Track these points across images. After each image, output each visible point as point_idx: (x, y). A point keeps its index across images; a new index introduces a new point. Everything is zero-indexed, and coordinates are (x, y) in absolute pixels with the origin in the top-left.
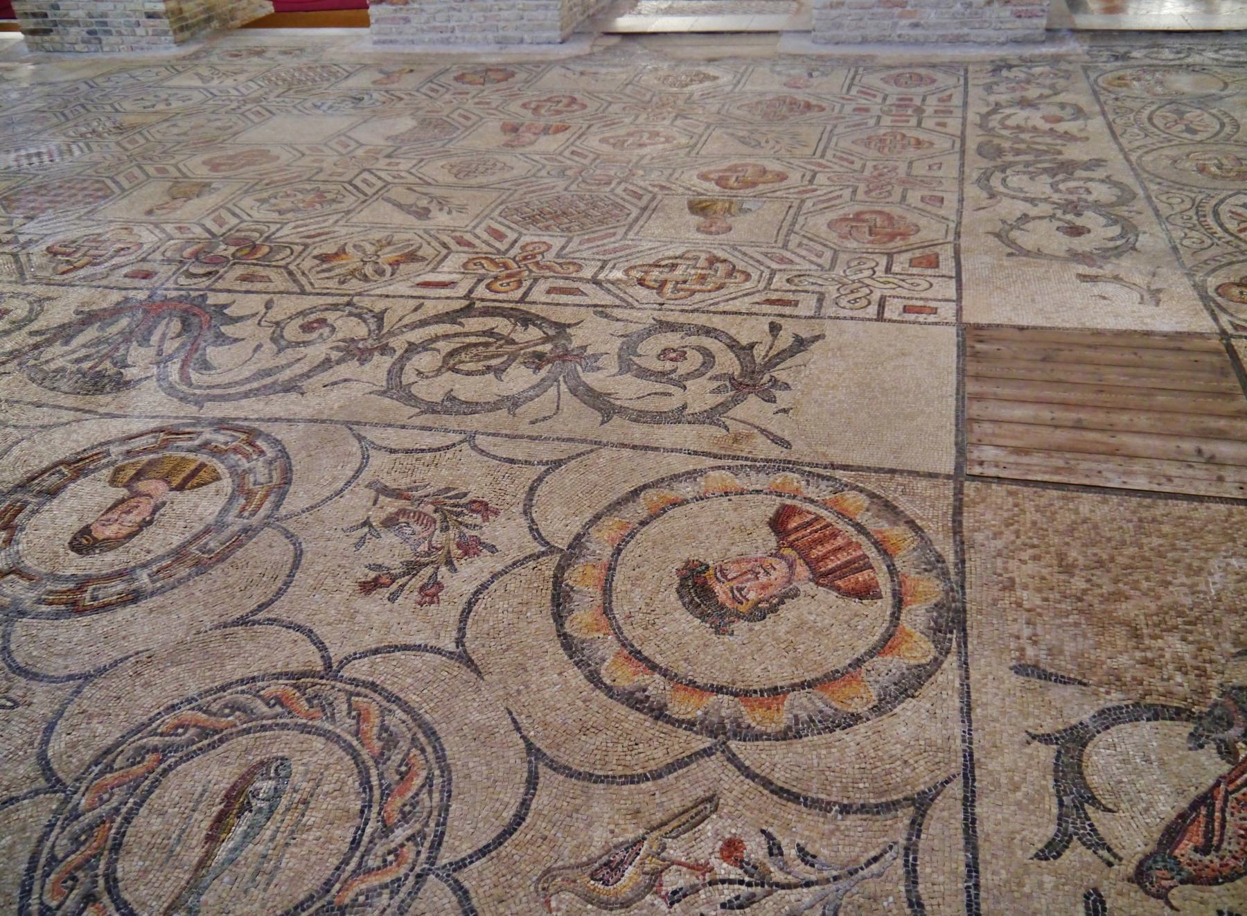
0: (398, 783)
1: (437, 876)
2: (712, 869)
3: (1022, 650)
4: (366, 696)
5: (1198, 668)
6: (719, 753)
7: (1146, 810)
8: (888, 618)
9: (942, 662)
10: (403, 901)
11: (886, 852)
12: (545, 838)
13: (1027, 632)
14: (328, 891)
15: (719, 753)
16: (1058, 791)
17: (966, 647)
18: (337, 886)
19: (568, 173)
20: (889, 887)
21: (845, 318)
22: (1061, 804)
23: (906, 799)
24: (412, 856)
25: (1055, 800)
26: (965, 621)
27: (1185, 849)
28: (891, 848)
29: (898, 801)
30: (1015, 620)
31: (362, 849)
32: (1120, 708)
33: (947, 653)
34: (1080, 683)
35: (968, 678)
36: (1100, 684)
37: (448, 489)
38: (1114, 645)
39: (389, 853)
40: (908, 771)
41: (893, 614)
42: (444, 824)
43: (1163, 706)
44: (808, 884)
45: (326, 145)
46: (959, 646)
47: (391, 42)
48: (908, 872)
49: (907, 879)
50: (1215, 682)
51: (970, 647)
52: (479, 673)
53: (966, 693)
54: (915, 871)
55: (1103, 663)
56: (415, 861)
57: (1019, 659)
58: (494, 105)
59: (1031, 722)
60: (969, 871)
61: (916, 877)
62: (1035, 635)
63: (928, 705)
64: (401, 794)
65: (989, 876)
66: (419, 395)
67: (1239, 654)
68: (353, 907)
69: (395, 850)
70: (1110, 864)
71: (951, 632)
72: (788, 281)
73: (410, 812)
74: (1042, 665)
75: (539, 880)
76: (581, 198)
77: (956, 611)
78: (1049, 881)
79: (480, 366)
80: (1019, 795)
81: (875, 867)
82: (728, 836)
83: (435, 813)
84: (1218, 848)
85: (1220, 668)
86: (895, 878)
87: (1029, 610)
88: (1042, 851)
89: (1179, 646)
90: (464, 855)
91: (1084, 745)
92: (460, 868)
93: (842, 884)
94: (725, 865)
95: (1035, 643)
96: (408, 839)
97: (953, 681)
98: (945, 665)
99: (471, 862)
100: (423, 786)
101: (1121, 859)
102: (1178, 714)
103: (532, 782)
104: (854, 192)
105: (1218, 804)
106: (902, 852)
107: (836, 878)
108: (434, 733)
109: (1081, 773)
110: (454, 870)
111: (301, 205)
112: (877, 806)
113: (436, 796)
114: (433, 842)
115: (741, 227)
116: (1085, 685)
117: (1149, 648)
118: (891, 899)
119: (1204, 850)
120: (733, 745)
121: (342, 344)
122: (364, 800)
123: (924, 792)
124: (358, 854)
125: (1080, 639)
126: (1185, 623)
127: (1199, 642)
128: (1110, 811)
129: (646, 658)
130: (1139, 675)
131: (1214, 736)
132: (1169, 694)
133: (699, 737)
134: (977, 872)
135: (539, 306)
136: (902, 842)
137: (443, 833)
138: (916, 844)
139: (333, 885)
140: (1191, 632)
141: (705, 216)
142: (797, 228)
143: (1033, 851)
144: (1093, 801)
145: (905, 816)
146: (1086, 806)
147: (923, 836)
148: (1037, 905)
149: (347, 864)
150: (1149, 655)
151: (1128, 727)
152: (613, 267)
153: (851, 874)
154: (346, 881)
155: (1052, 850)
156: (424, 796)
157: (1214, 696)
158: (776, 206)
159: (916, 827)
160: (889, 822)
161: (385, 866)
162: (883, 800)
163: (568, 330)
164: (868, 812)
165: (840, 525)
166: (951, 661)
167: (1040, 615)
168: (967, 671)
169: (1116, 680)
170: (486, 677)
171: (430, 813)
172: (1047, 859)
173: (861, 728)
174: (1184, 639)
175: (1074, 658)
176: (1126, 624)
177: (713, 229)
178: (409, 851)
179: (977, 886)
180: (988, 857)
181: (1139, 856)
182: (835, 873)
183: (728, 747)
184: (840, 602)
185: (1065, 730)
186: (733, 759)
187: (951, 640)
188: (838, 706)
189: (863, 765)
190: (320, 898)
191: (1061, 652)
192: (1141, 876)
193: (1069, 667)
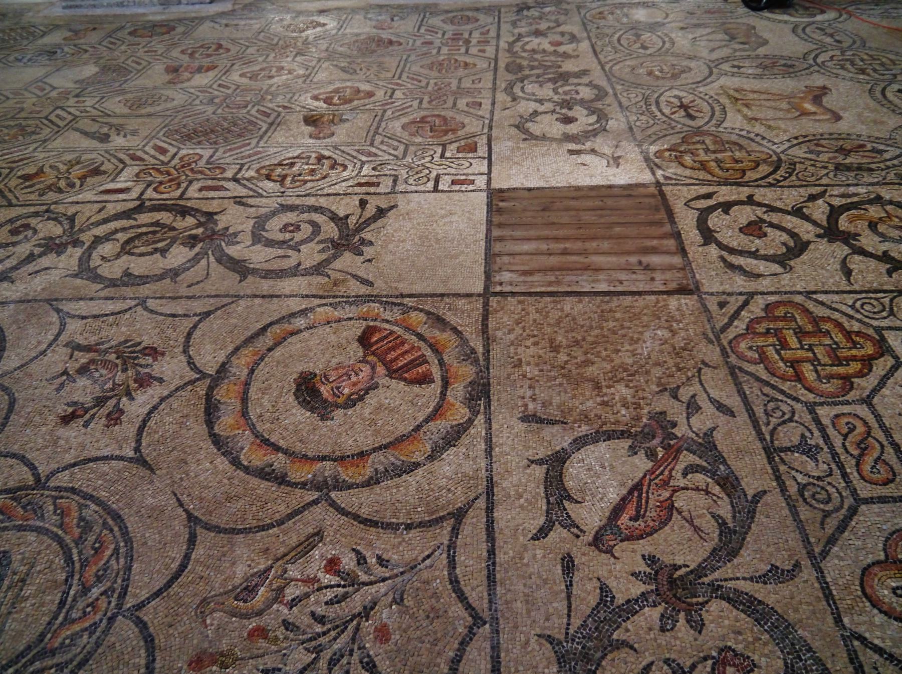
0: (93, 556)
1: (124, 616)
2: (319, 580)
3: (526, 406)
4: (68, 498)
5: (635, 403)
7: (602, 499)
8: (438, 395)
9: (474, 420)
10: (99, 638)
11: (435, 551)
12: (202, 578)
13: (529, 393)
14: (42, 641)
16: (547, 495)
18: (49, 636)
19: (216, 101)
20: (437, 573)
21: (412, 192)
22: (548, 503)
23: (448, 514)
24: (105, 605)
25: (545, 500)
26: (489, 391)
27: (624, 520)
28: (439, 547)
29: (444, 516)
30: (522, 387)
31: (67, 606)
32: (587, 435)
34: (563, 423)
36: (575, 422)
37: (126, 341)
38: (583, 395)
39: (88, 606)
41: (441, 393)
42: (128, 579)
43: (613, 431)
44: (384, 580)
45: (26, 90)
46: (485, 408)
47: (77, 6)
48: (449, 562)
49: (449, 566)
50: (645, 411)
51: (492, 408)
53: (489, 440)
54: (454, 560)
55: (577, 408)
56: (107, 609)
57: (524, 412)
58: (159, 53)
59: (531, 452)
60: (489, 555)
61: (455, 564)
62: (535, 395)
64: (96, 564)
65: (502, 556)
66: (103, 275)
67: (661, 391)
68: (61, 648)
69: (93, 603)
70: (578, 536)
71: (480, 400)
72: (373, 169)
73: (103, 575)
74: (538, 414)
75: (198, 607)
76: (225, 119)
77: (484, 385)
78: (539, 553)
79: (149, 249)
80: (522, 501)
81: (428, 562)
82: (330, 556)
83: (122, 573)
84: (644, 516)
85: (649, 402)
86: (441, 567)
87: (530, 379)
88: (536, 534)
89: (624, 391)
90: (143, 598)
91: (564, 463)
92: (140, 608)
93: (406, 576)
94: (328, 576)
95: (534, 400)
96: (102, 594)
97: (481, 432)
98: (475, 422)
99: (149, 603)
100: (112, 555)
101: (585, 532)
102: (623, 435)
103: (192, 540)
104: (421, 102)
105: (645, 490)
106: (446, 549)
107: (402, 573)
108: (120, 517)
109: (562, 481)
110: (136, 610)
111: (7, 138)
112: (429, 521)
113: (122, 561)
114: (120, 593)
115: (341, 133)
116: (565, 423)
117: (606, 394)
118: (438, 581)
119: (635, 519)
120: (333, 495)
121: (42, 241)
122: (68, 572)
123: (461, 508)
124: (64, 611)
125: (562, 394)
126: (628, 375)
127: (636, 387)
128: (579, 502)
129: (273, 444)
130: (599, 412)
131: (643, 446)
132: (617, 422)
134: (494, 554)
135: (194, 201)
136: (446, 542)
137: (127, 586)
138: (455, 543)
139: (45, 636)
140: (631, 381)
141: (316, 126)
142: (380, 130)
143: (530, 536)
144: (570, 498)
145: (448, 526)
146: (564, 501)
147: (460, 537)
148: (532, 570)
149: (56, 619)
150: (606, 399)
151: (591, 447)
152: (248, 169)
153: (412, 568)
154: (55, 631)
155: (543, 533)
156: (113, 562)
157: (644, 420)
158: (365, 116)
159: (455, 532)
160: (438, 531)
161: (85, 616)
162: (434, 517)
163: (215, 217)
164: (423, 527)
165: (407, 336)
166: (480, 419)
167: (538, 381)
168: (490, 424)
169: (585, 418)
170: (157, 472)
171: (118, 573)
172: (538, 539)
173: (420, 471)
174: (627, 386)
175: (558, 407)
176: (591, 380)
177: (321, 135)
178: (103, 603)
179: (494, 564)
180: (502, 544)
181: (597, 528)
182: (401, 570)
185: (552, 455)
186: (333, 504)
187: (480, 405)
188: (405, 459)
190: (36, 647)
191: (551, 404)
192: (597, 542)
193: (556, 413)
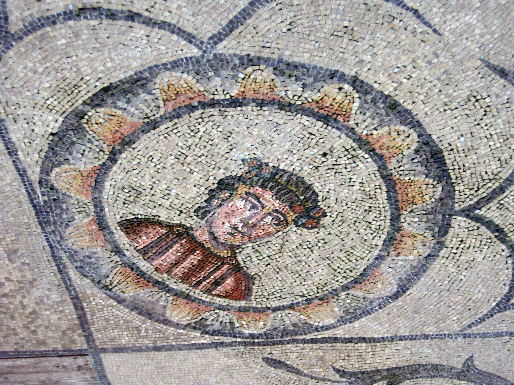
6: (205, 40)
8: (105, 205)
9: (42, 172)
15: (205, 40)
17: (27, 191)
23: (21, 38)
26: (37, 214)
29: (26, 34)
33: (40, 182)
35: (14, 162)
40: (30, 65)
41: (102, 210)
51: (24, 191)
52: (489, 65)
63: (36, 129)
71: (45, 202)
77: (47, 223)
98: (38, 169)
112: (43, 25)
120: (195, 52)
133: (231, 52)
164: (48, 18)
165: (183, 287)
170: (479, 63)
183: (200, 48)
184: (154, 212)
186: (190, 38)
187: (43, 195)
188: (114, 111)
189: (69, 60)
